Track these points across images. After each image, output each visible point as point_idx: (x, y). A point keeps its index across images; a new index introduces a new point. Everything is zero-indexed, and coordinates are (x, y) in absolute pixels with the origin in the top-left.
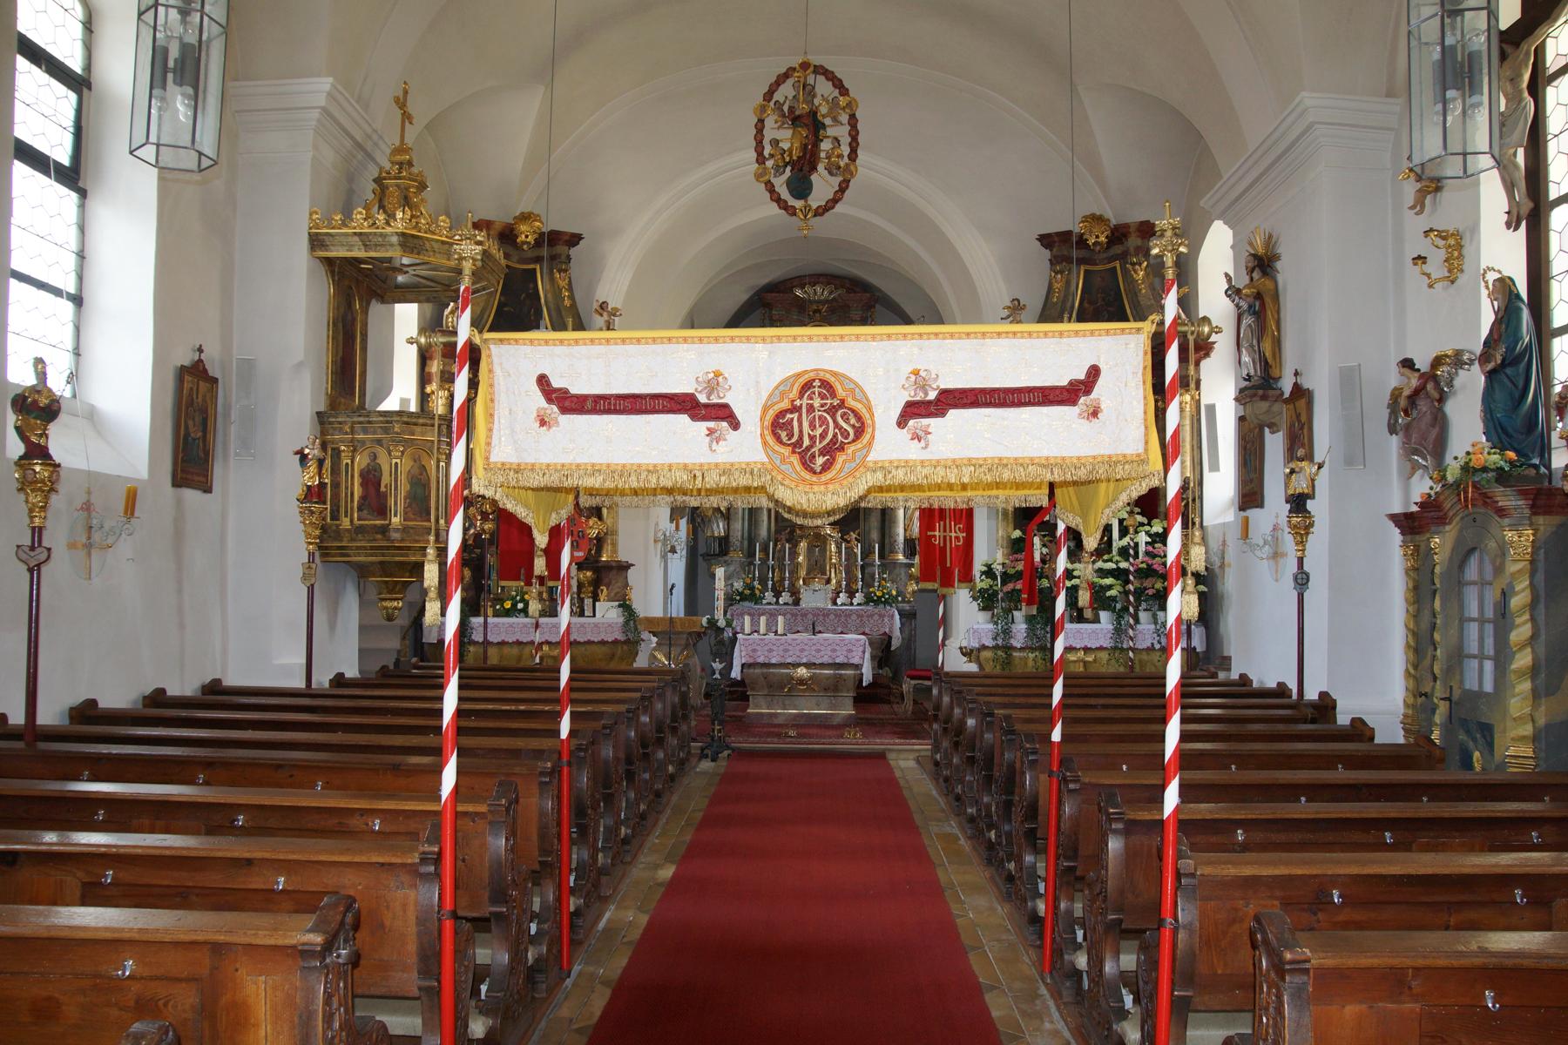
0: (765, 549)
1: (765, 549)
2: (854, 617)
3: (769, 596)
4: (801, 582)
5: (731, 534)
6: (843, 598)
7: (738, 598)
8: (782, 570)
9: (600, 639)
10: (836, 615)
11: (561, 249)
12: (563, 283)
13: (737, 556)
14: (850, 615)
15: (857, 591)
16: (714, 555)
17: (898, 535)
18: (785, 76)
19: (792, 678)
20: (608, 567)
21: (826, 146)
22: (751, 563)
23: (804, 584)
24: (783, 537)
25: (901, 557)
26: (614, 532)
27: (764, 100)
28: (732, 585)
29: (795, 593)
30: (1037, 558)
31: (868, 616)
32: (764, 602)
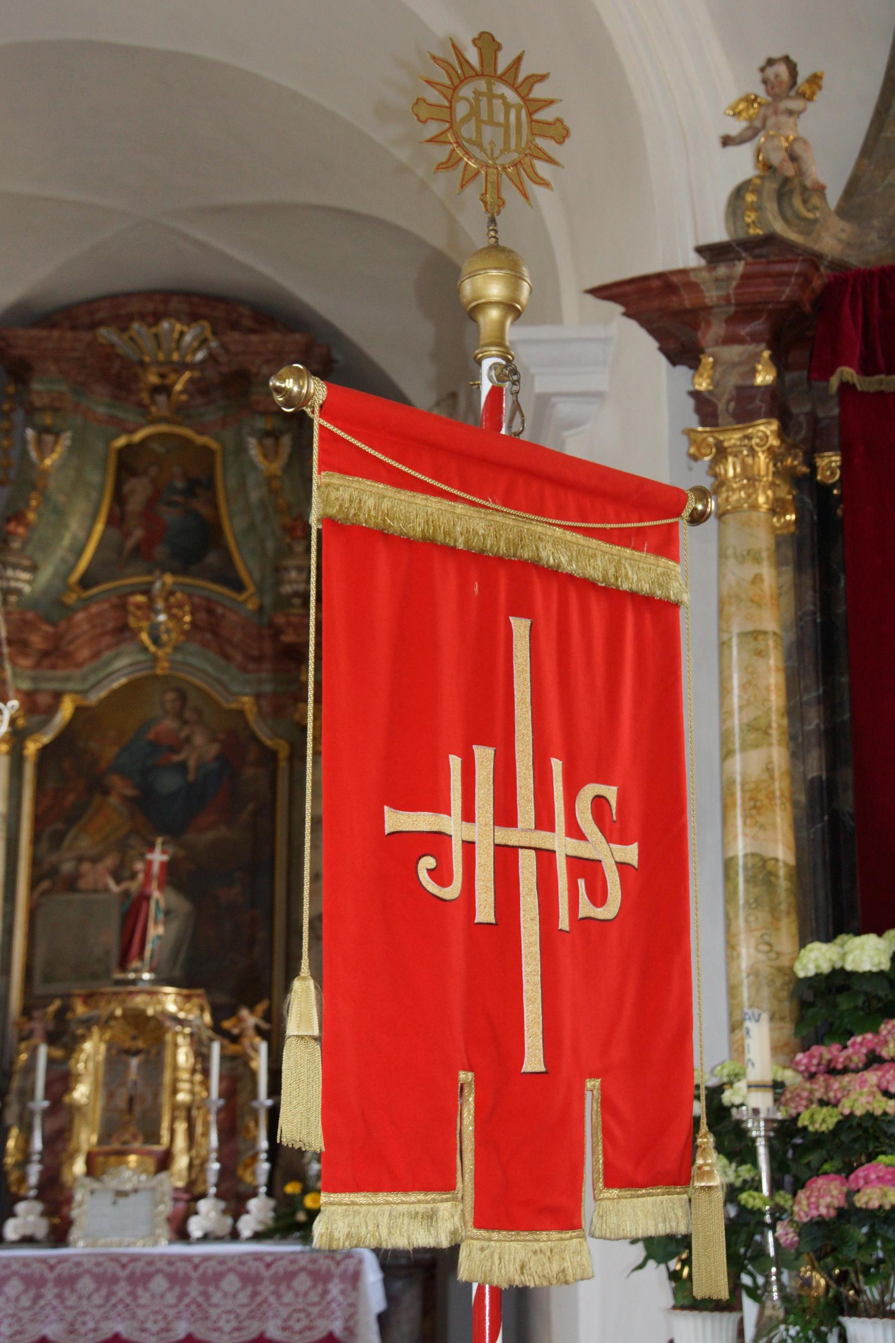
2: (231, 1283)
4: (79, 1167)
10: (174, 1279)
14: (217, 1278)
24: (38, 1026)
31: (277, 1279)
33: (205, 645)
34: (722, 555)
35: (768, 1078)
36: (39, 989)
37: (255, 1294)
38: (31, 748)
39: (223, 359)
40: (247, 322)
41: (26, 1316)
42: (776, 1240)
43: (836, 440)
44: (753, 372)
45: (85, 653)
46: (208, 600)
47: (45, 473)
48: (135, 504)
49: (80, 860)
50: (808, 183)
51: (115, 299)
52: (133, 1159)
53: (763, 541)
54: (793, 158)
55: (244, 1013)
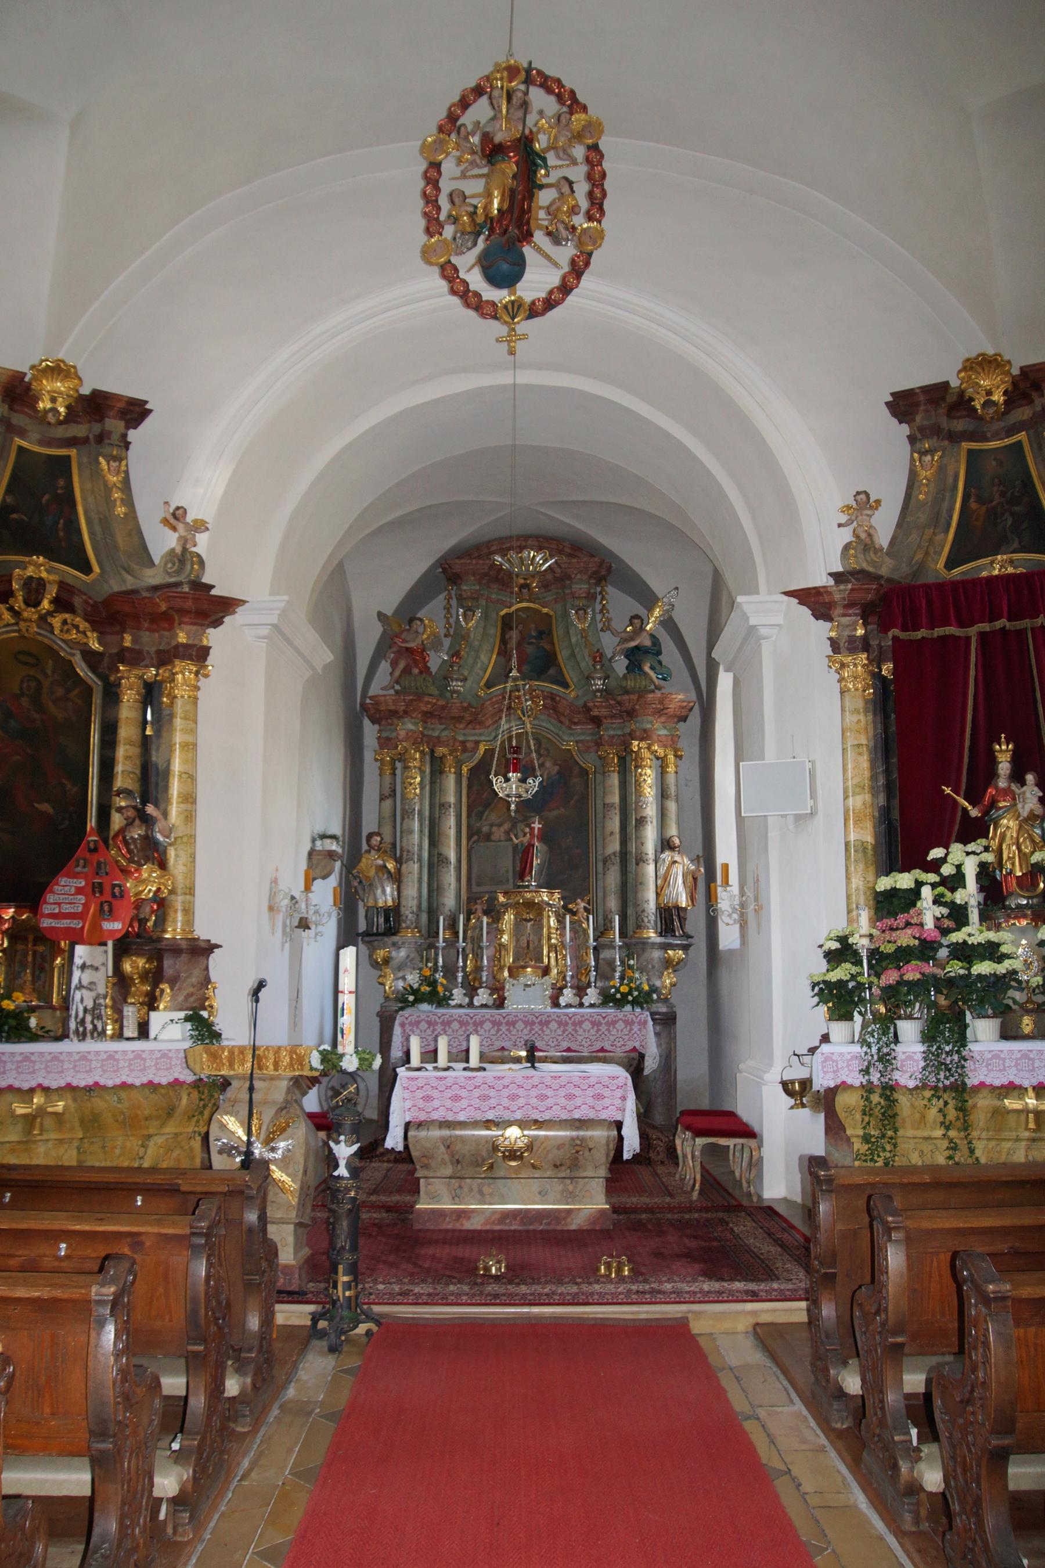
0: (452, 926)
1: (452, 926)
2: (587, 1025)
3: (458, 995)
4: (506, 974)
5: (403, 903)
6: (568, 996)
7: (411, 998)
8: (478, 957)
9: (145, 1080)
10: (560, 1023)
11: (114, 425)
12: (113, 479)
13: (409, 936)
14: (581, 1023)
15: (589, 985)
16: (377, 934)
17: (647, 901)
18: (478, 91)
19: (495, 1148)
20: (175, 949)
21: (545, 197)
22: (432, 946)
23: (510, 976)
24: (479, 907)
25: (652, 935)
26: (190, 891)
27: (441, 129)
28: (404, 978)
29: (498, 990)
30: (929, 923)
31: (608, 1024)
32: (452, 1003)
33: (549, 716)
34: (843, 710)
35: (868, 933)
36: (475, 889)
37: (598, 1030)
38: (465, 770)
39: (558, 570)
40: (567, 550)
41: (494, 1038)
42: (871, 994)
43: (890, 655)
44: (856, 630)
45: (490, 721)
46: (552, 694)
47: (469, 630)
48: (513, 643)
49: (492, 825)
50: (877, 546)
51: (500, 540)
52: (529, 970)
53: (860, 704)
54: (870, 535)
55: (579, 901)
